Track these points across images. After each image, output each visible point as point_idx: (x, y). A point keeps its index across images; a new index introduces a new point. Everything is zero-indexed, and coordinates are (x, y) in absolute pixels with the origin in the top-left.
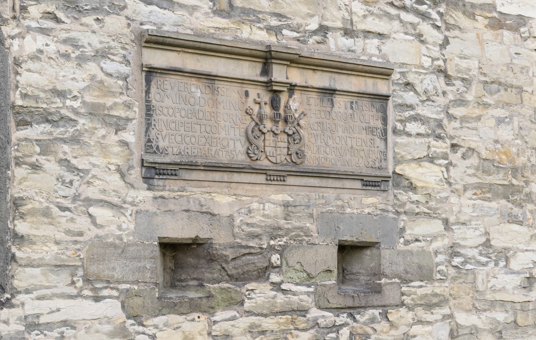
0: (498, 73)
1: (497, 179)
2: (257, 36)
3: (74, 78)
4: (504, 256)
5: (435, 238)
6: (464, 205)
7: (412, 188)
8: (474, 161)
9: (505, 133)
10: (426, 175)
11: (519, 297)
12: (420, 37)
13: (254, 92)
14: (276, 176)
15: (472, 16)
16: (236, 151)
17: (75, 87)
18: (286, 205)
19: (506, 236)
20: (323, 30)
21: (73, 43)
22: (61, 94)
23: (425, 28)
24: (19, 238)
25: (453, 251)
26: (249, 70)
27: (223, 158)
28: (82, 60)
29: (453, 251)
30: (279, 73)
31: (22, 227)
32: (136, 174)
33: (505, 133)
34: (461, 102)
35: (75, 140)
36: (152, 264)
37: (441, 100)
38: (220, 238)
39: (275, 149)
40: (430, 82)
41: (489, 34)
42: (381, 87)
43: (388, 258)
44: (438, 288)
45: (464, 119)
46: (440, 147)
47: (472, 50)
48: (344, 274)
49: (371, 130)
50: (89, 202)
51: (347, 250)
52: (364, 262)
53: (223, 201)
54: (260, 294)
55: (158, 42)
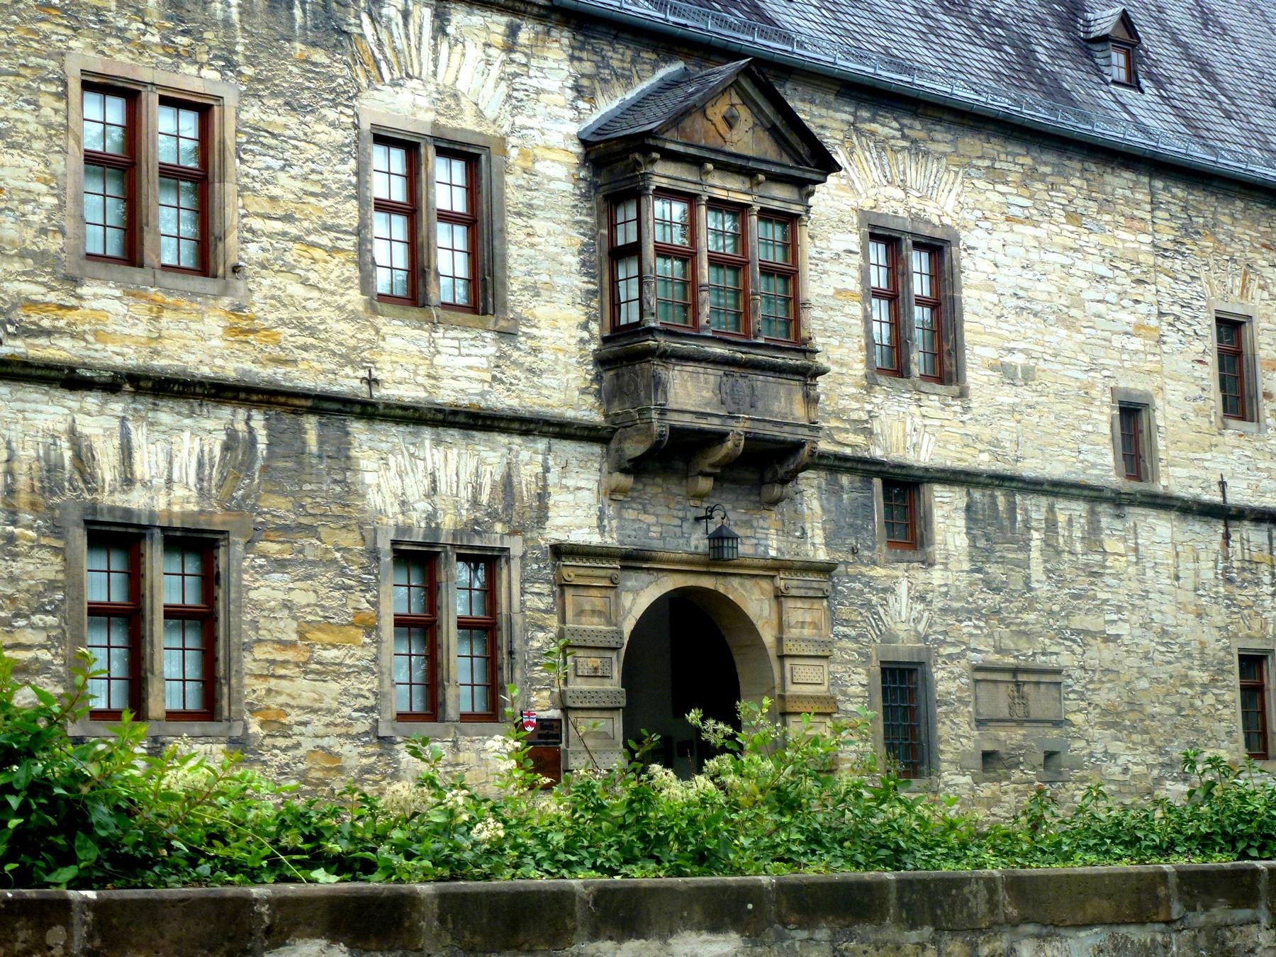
0: (1107, 665)
1: (1109, 719)
2: (1010, 661)
3: (953, 686)
4: (1113, 757)
5: (1083, 749)
6: (1096, 732)
7: (1073, 725)
8: (1098, 710)
9: (1113, 696)
10: (1078, 718)
11: (1121, 778)
12: (1073, 652)
13: (1011, 686)
14: (1020, 723)
15: (1095, 638)
16: (1005, 713)
17: (953, 690)
18: (1024, 735)
19: (1116, 747)
20: (1034, 654)
21: (952, 672)
22: (949, 693)
23: (1075, 647)
24: (941, 751)
25: (1091, 755)
26: (1007, 677)
27: (1001, 716)
28: (955, 679)
29: (1091, 755)
30: (1022, 678)
31: (942, 747)
32: (973, 725)
33: (1113, 696)
34: (1091, 682)
35: (954, 712)
36: (978, 761)
37: (1083, 682)
38: (1002, 750)
39: (1019, 711)
40: (1078, 673)
41: (1102, 646)
42: (1058, 679)
43: (1064, 758)
44: (1085, 773)
45: (1094, 690)
46: (1083, 704)
47: (1096, 655)
48: (1045, 766)
49: (1054, 699)
50: (960, 736)
51: (1050, 755)
52: (1055, 759)
53: (1002, 734)
54: (1016, 774)
55: (978, 669)
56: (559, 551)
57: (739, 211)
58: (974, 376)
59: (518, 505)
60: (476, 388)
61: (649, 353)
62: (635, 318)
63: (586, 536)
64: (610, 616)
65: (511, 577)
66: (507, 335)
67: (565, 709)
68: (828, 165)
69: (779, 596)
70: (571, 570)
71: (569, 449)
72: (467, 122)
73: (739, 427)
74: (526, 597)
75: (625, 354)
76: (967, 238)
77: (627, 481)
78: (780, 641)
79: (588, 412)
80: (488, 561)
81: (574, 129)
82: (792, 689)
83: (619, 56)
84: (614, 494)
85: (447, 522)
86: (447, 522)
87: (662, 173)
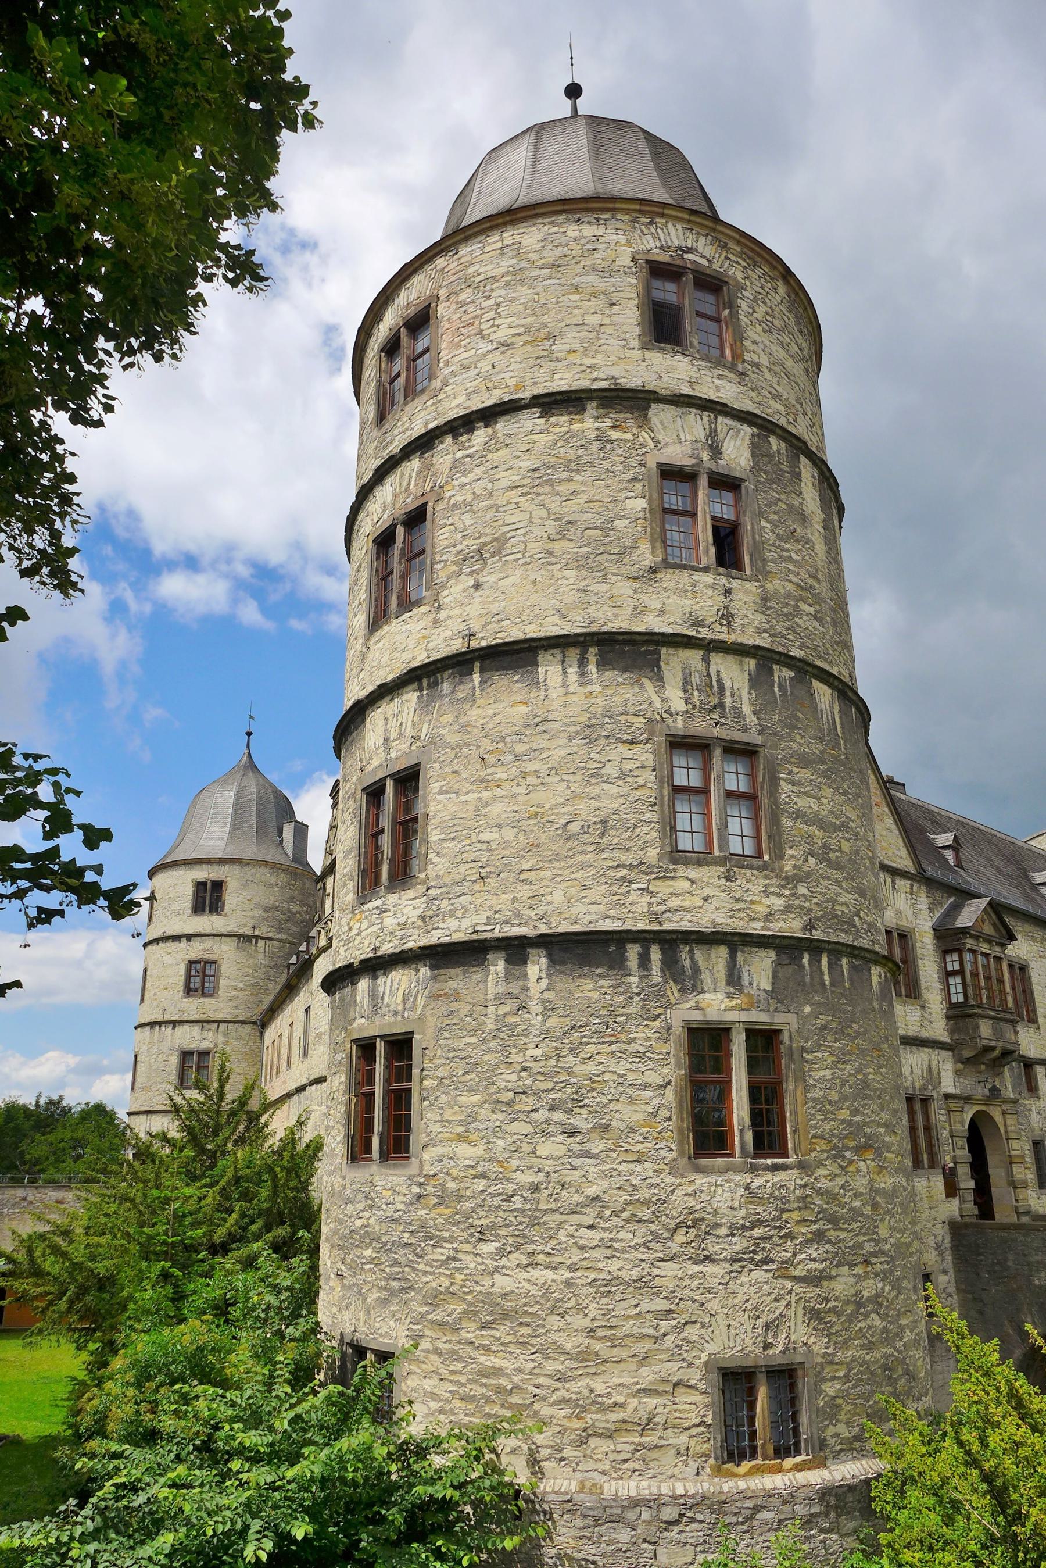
56: (947, 1096)
57: (987, 955)
58: (1041, 1020)
59: (932, 1077)
60: (917, 1029)
61: (975, 1014)
62: (961, 999)
63: (951, 1090)
64: (962, 1123)
65: (934, 1107)
66: (923, 1007)
67: (955, 1163)
68: (1012, 938)
69: (1004, 1113)
70: (953, 1104)
71: (945, 1054)
72: (904, 923)
73: (1000, 1044)
74: (938, 1115)
75: (959, 1015)
76: (1032, 964)
77: (960, 1066)
78: (1006, 1132)
79: (946, 1038)
80: (925, 1101)
81: (930, 924)
82: (1013, 1153)
83: (938, 895)
84: (958, 1073)
85: (917, 1085)
86: (917, 1085)
87: (969, 943)
